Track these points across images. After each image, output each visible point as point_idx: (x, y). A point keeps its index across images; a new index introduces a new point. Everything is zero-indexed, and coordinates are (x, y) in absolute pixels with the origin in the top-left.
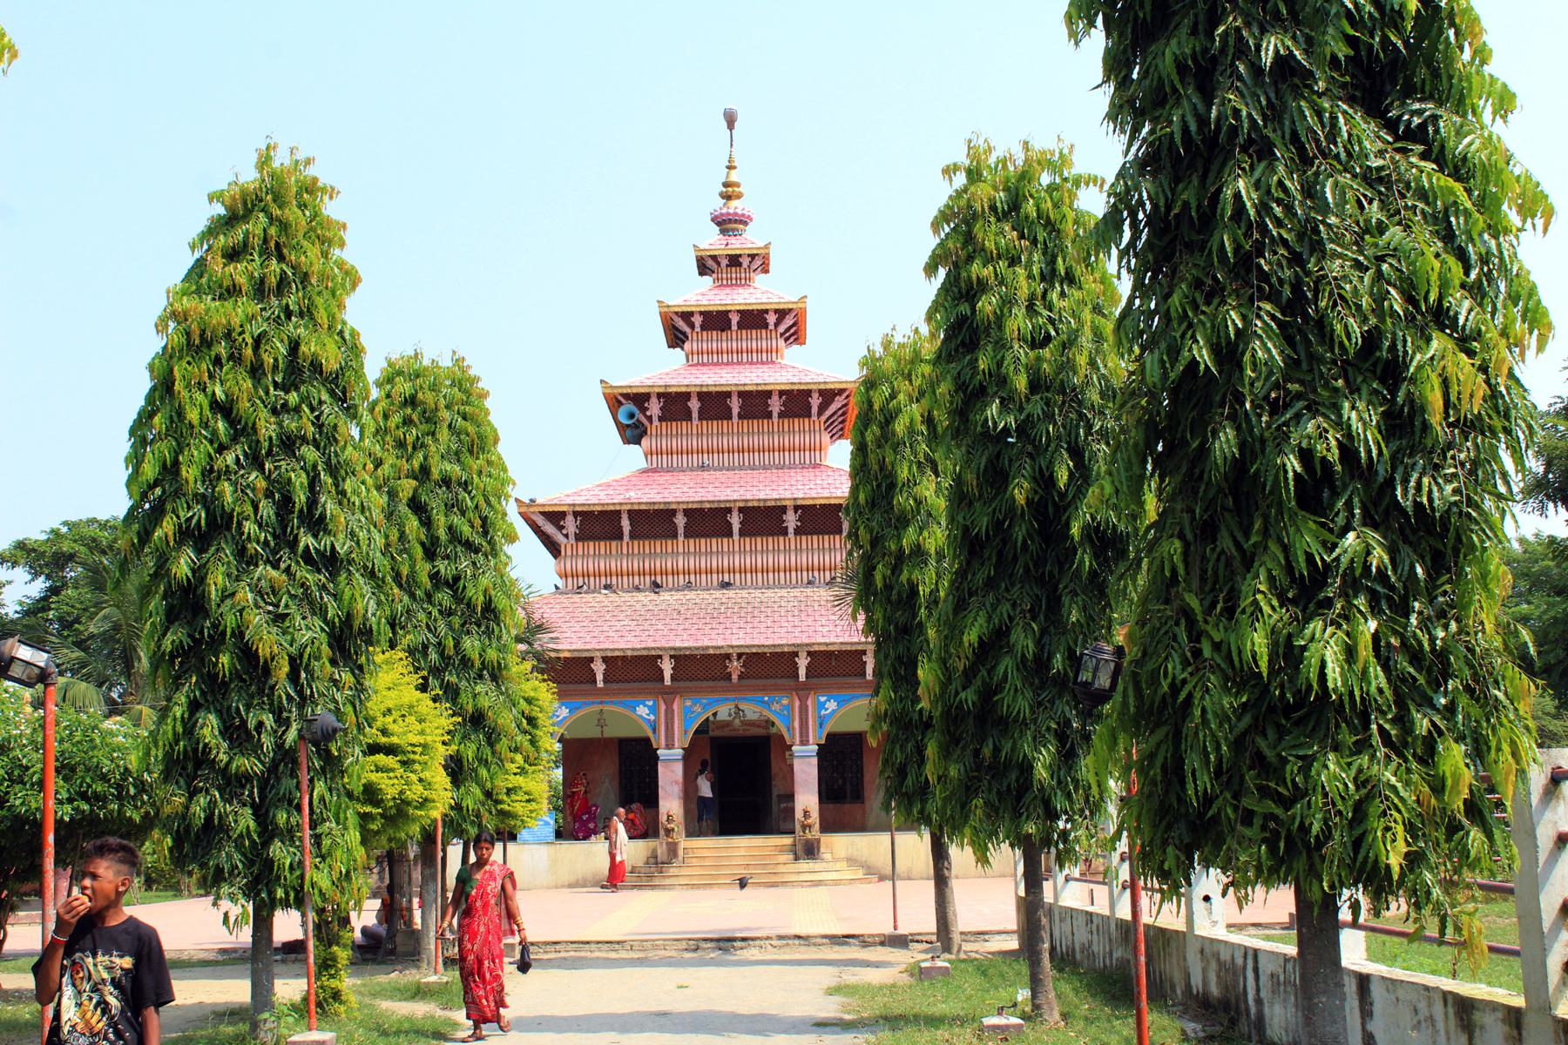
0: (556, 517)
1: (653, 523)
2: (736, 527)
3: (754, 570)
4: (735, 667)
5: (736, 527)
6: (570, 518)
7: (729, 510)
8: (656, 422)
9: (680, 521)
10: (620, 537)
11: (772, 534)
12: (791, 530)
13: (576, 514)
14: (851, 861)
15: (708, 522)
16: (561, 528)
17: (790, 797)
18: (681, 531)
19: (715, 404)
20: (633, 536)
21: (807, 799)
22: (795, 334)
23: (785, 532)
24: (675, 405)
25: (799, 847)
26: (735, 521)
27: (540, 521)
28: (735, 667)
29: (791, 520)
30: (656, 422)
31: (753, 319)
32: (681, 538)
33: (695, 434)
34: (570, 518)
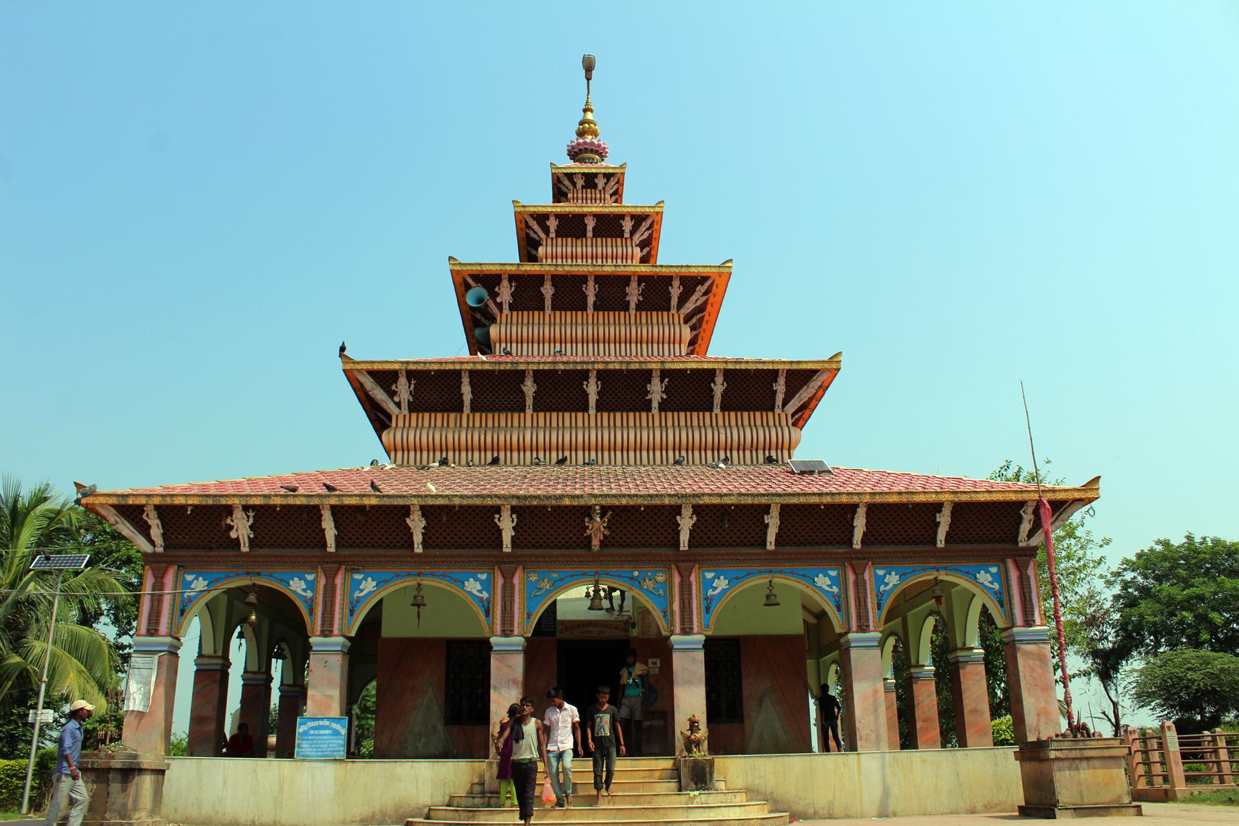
0: (386, 378)
2: (593, 399)
3: (612, 448)
5: (593, 399)
6: (403, 380)
7: (585, 375)
8: (506, 311)
9: (529, 388)
10: (460, 409)
11: (634, 409)
12: (655, 404)
13: (411, 374)
14: (752, 793)
15: (560, 391)
16: (392, 394)
18: (529, 402)
20: (474, 409)
23: (647, 407)
25: (684, 772)
26: (592, 389)
27: (369, 383)
29: (656, 390)
30: (506, 311)
32: (529, 411)
34: (403, 380)
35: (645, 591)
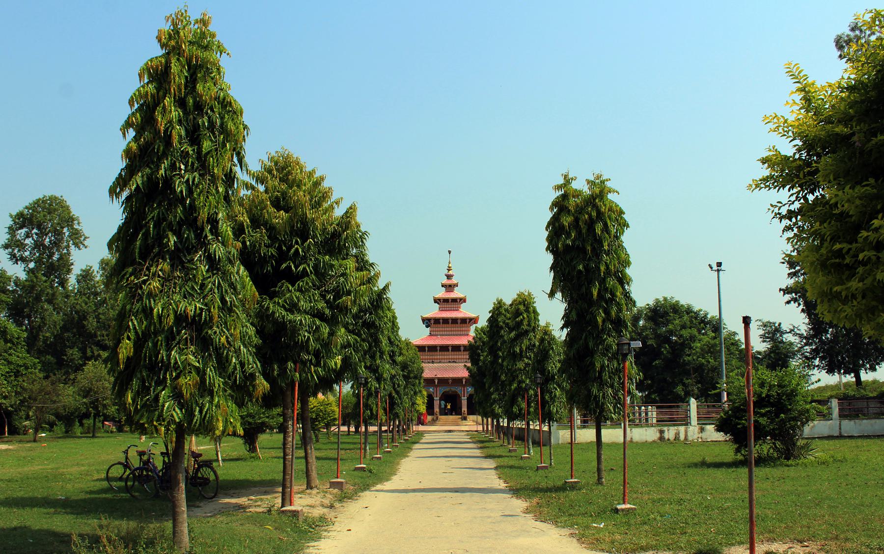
1: (432, 349)
4: (450, 381)
15: (444, 348)
17: (461, 408)
19: (446, 321)
21: (464, 409)
22: (465, 301)
24: (437, 321)
28: (450, 381)
31: (454, 300)
33: (441, 327)
35: (458, 390)
